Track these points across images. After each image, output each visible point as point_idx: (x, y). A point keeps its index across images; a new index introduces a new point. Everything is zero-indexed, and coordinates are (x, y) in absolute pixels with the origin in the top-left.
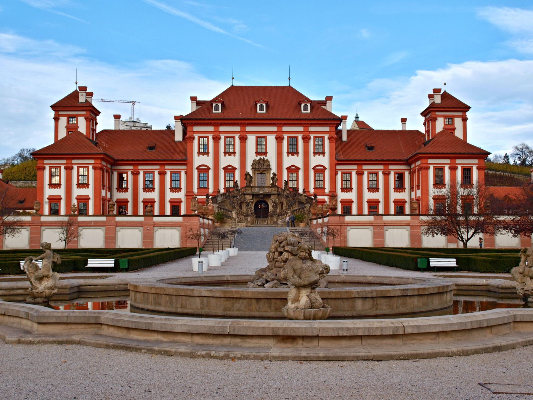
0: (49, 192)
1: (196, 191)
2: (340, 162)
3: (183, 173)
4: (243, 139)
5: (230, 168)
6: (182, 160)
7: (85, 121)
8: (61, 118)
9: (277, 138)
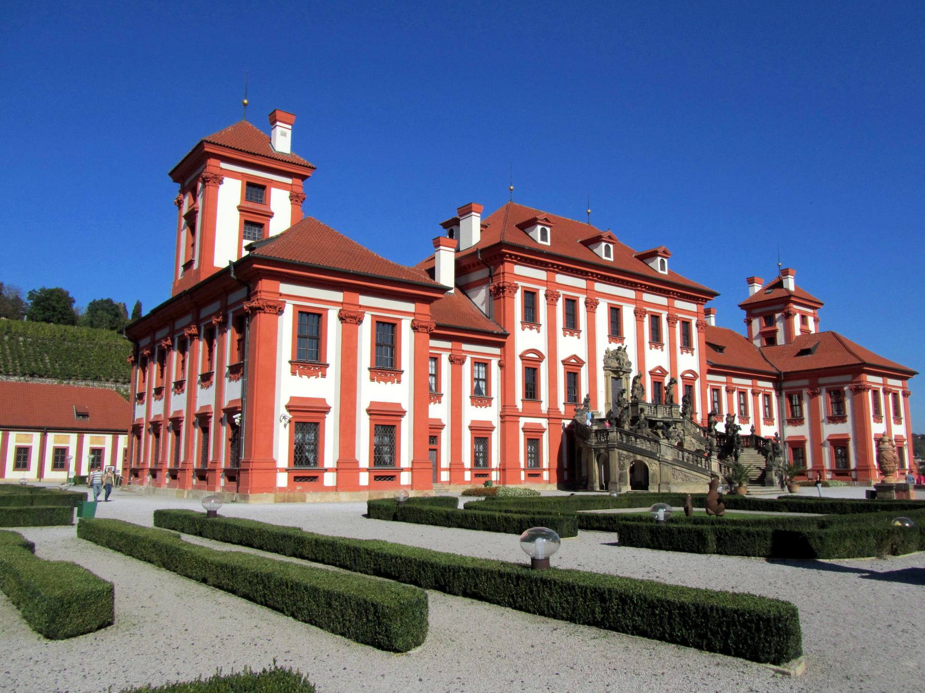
0: (290, 386)
1: (519, 405)
2: (715, 369)
3: (494, 364)
4: (591, 305)
5: (573, 361)
6: (497, 335)
7: (288, 203)
8: (226, 180)
9: (635, 313)
